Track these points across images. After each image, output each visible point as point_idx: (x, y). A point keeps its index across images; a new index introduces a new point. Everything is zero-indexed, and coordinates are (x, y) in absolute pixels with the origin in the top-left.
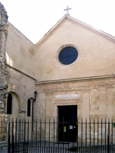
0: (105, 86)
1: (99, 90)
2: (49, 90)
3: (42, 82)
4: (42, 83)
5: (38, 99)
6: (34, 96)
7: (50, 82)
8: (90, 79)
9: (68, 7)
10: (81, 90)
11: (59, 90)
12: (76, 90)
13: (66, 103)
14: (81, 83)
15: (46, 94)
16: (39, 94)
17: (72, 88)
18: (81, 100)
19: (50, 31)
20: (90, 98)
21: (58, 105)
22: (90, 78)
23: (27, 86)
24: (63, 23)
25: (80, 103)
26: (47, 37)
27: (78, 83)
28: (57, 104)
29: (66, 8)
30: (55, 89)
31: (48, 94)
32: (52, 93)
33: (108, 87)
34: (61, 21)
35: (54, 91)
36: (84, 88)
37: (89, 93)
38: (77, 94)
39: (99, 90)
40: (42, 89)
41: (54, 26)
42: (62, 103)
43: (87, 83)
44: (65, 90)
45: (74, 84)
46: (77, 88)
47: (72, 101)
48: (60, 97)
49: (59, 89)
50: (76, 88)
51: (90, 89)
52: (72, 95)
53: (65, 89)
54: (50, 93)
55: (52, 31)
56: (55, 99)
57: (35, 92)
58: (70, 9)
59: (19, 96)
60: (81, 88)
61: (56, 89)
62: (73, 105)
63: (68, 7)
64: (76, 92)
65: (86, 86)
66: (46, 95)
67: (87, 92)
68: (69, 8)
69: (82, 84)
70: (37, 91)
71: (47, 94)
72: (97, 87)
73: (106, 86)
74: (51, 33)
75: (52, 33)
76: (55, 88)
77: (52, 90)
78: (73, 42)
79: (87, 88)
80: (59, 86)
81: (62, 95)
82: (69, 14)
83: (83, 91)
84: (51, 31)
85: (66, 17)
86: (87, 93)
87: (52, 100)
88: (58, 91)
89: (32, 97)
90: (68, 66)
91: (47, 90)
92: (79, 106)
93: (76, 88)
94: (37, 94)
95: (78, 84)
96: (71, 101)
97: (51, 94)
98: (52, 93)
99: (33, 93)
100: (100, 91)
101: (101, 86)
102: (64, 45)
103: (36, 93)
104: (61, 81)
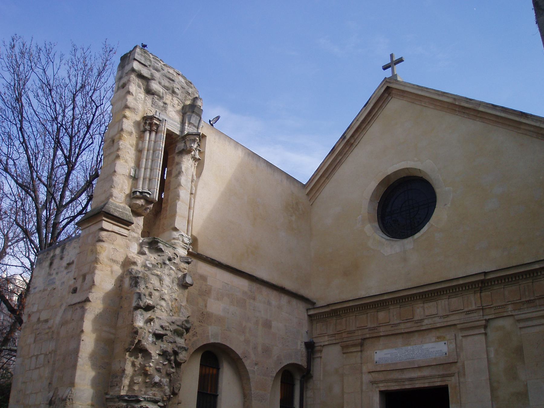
0: (537, 302)
1: (519, 321)
2: (350, 332)
3: (328, 305)
4: (327, 310)
5: (318, 370)
6: (305, 359)
7: (351, 304)
8: (482, 282)
10: (455, 325)
11: (382, 331)
12: (438, 325)
13: (411, 379)
14: (454, 300)
15: (343, 347)
16: (321, 351)
17: (426, 322)
18: (459, 364)
19: (343, 137)
20: (492, 355)
21: (383, 389)
22: (482, 277)
23: (274, 324)
24: (381, 106)
25: (456, 375)
26: (340, 158)
27: (443, 301)
28: (381, 385)
29: (389, 61)
30: (371, 329)
31: (347, 347)
32: (362, 345)
34: (374, 101)
35: (368, 336)
37: (486, 334)
38: (443, 342)
39: (519, 321)
40: (331, 332)
41: (356, 119)
42: (396, 381)
44: (403, 328)
45: (431, 304)
46: (441, 317)
48: (389, 356)
49: (382, 329)
51: (487, 317)
52: (425, 346)
53: (402, 326)
54: (355, 345)
55: (352, 136)
56: (371, 367)
57: (306, 344)
58: (400, 60)
59: (244, 360)
60: (454, 319)
61: (374, 328)
62: (431, 385)
63: (392, 56)
64: (438, 333)
65: (470, 308)
66: (344, 353)
67: (476, 331)
68: (395, 59)
69: (456, 302)
70: (315, 340)
71: (345, 348)
72: (510, 308)
74: (348, 141)
75: (352, 141)
76: (369, 326)
77: (360, 333)
78: (416, 159)
79: (475, 316)
80: (382, 315)
81: (393, 351)
83: (462, 329)
84: (348, 137)
85: (388, 88)
86: (476, 338)
87: (365, 369)
88: (381, 334)
89: (296, 362)
90: (408, 243)
91: (344, 335)
93: (437, 320)
94: (317, 348)
96: (426, 373)
97: (359, 349)
98: (362, 344)
99: (299, 348)
101: (525, 306)
103: (310, 346)
104: (385, 297)
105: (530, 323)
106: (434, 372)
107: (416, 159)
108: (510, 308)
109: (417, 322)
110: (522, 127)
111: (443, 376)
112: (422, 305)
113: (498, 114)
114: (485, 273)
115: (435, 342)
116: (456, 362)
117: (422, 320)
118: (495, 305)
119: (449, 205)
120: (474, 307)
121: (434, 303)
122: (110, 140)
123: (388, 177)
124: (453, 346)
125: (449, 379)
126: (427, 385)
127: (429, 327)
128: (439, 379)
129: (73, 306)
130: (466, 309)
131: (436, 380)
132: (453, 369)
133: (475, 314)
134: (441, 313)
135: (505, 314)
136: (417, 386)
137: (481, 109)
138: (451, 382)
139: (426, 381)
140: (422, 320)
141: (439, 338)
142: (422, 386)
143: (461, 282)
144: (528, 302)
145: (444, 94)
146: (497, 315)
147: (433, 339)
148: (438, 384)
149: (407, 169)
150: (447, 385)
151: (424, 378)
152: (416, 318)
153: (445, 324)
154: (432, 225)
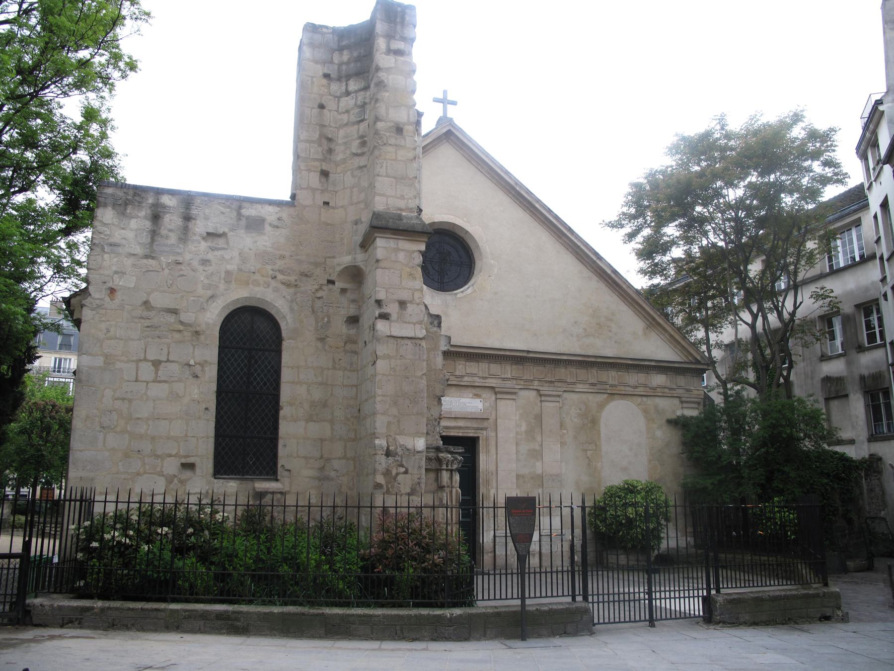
0: (556, 383)
8: (521, 357)
9: (445, 92)
10: (492, 388)
12: (477, 384)
17: (466, 379)
22: (525, 354)
24: (435, 145)
25: (489, 429)
27: (484, 364)
33: (565, 389)
36: (500, 381)
38: (478, 400)
43: (509, 371)
45: (472, 364)
47: (464, 420)
50: (479, 380)
52: (463, 400)
60: (492, 382)
62: (465, 435)
63: (445, 92)
65: (506, 376)
68: (449, 98)
69: (495, 368)
72: (536, 383)
73: (559, 384)
78: (465, 219)
79: (509, 384)
82: (451, 120)
86: (508, 402)
92: (487, 439)
93: (476, 379)
95: (484, 365)
96: (461, 423)
100: (543, 398)
101: (547, 385)
102: (436, 221)
105: (549, 399)
106: (469, 424)
107: (465, 219)
108: (536, 383)
109: (457, 377)
110: (564, 238)
111: (478, 429)
112: (464, 363)
113: (551, 218)
114: (528, 352)
115: (472, 398)
116: (488, 419)
117: (462, 376)
118: (525, 378)
119: (493, 278)
120: (509, 376)
121: (477, 364)
122: (392, 124)
123: (434, 223)
124: (487, 404)
125: (481, 432)
126: (460, 435)
127: (469, 384)
128: (473, 431)
129: (399, 340)
130: (503, 376)
131: (470, 431)
132: (485, 424)
133: (509, 382)
134: (480, 374)
135: (532, 387)
136: (452, 434)
137: (537, 205)
138: (482, 435)
139: (461, 431)
140: (462, 376)
141: (477, 396)
142: (456, 434)
143: (508, 353)
144: (551, 382)
145: (507, 173)
146: (525, 387)
147: (471, 395)
148: (471, 435)
149: (455, 224)
150: (478, 438)
151: (460, 428)
152: (457, 373)
153: (483, 385)
154: (475, 291)
